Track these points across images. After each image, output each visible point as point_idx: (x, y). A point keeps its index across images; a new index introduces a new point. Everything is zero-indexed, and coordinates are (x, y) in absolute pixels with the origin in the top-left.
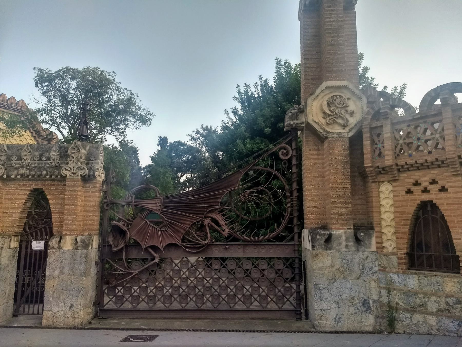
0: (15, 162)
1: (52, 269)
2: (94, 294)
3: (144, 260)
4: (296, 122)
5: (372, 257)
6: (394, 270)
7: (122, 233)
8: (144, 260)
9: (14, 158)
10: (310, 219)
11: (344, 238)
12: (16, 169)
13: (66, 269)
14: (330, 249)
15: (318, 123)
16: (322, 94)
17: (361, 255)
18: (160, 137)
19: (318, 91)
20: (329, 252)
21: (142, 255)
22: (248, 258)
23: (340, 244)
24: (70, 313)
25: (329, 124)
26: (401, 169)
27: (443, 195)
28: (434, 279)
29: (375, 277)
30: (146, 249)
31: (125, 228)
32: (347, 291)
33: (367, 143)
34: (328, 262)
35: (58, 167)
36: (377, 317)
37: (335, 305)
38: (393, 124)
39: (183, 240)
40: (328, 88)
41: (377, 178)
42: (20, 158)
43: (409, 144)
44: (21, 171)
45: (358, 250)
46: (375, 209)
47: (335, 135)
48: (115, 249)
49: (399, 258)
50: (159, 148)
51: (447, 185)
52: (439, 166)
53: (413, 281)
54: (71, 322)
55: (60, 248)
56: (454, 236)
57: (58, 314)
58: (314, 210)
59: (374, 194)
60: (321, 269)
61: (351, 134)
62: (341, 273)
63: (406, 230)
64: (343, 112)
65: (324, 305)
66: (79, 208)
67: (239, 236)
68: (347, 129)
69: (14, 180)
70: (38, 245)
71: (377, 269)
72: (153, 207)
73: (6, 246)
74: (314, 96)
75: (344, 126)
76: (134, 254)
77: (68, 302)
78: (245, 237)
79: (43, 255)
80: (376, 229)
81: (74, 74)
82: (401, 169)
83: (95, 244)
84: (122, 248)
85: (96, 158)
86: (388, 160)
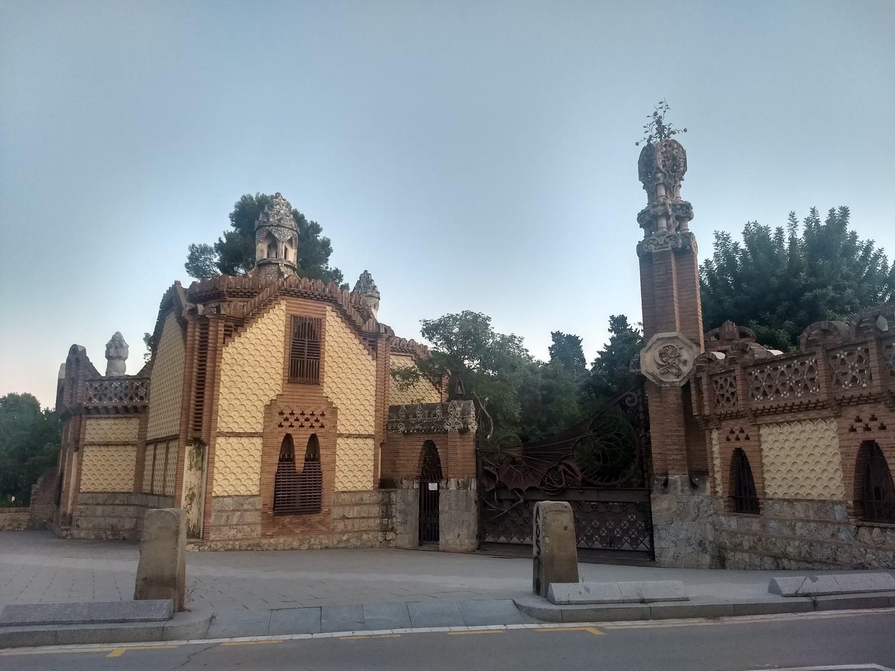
0: (412, 420)
1: (443, 505)
2: (476, 528)
3: (513, 501)
4: (637, 370)
5: (706, 501)
6: (722, 513)
7: (494, 477)
8: (513, 501)
9: (411, 416)
10: (657, 465)
11: (680, 483)
12: (413, 425)
13: (453, 505)
14: (667, 493)
15: (652, 374)
16: (655, 346)
17: (696, 499)
18: (612, 317)
19: (649, 344)
20: (665, 496)
21: (509, 496)
22: (602, 502)
23: (676, 488)
24: (458, 541)
25: (663, 374)
26: (722, 418)
27: (747, 443)
28: (747, 520)
29: (710, 519)
30: (513, 491)
31: (494, 472)
32: (684, 532)
33: (693, 392)
34: (665, 505)
35: (442, 422)
36: (713, 557)
37: (672, 545)
38: (711, 376)
39: (542, 484)
40: (658, 339)
41: (707, 425)
42: (415, 416)
43: (723, 395)
44: (417, 427)
45: (693, 494)
46: (709, 455)
47: (668, 385)
48: (488, 490)
49: (725, 502)
50: (613, 334)
51: (750, 434)
52: (743, 417)
53: (733, 523)
54: (459, 548)
55: (448, 488)
56: (755, 480)
57: (450, 542)
58: (659, 457)
59: (708, 441)
60: (659, 511)
61: (683, 384)
62: (678, 515)
63: (727, 474)
64: (677, 361)
65: (663, 544)
66: (459, 456)
67: (591, 480)
68: (681, 378)
69: (413, 433)
70: (432, 487)
71: (712, 512)
72: (515, 454)
73: (410, 487)
74: (646, 348)
75: (678, 377)
76: (505, 495)
77: (456, 532)
78: (596, 482)
79: (436, 494)
80: (710, 474)
81: (453, 318)
82: (722, 418)
83: (474, 485)
84: (493, 491)
85: (469, 414)
86: (707, 412)
